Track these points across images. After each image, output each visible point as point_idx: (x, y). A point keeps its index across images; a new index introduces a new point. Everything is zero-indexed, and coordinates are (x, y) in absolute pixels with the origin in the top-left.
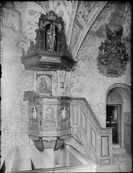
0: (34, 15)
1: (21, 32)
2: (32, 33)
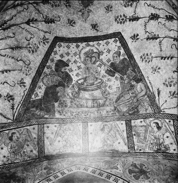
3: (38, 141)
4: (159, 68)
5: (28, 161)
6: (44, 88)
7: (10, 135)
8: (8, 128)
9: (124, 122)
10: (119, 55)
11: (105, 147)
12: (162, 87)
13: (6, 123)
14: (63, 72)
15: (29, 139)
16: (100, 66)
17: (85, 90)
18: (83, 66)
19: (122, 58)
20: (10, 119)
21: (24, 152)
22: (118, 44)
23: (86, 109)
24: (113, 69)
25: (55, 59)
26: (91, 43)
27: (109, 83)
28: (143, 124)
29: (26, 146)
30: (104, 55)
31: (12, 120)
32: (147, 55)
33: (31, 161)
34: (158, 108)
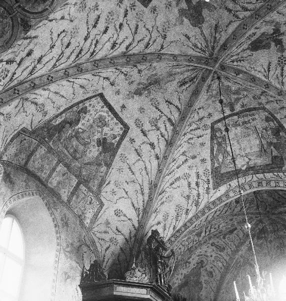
0: (119, 216)
1: (90, 229)
2: (104, 240)
4: (122, 171)
6: (63, 118)
9: (77, 181)
10: (114, 139)
11: (56, 189)
12: (112, 182)
14: (79, 116)
16: (98, 132)
17: (77, 138)
18: (91, 121)
19: (113, 141)
22: (121, 132)
23: (67, 153)
24: (102, 143)
25: (86, 105)
26: (110, 113)
27: (92, 148)
28: (86, 193)
30: (108, 128)
32: (125, 157)
34: (100, 191)
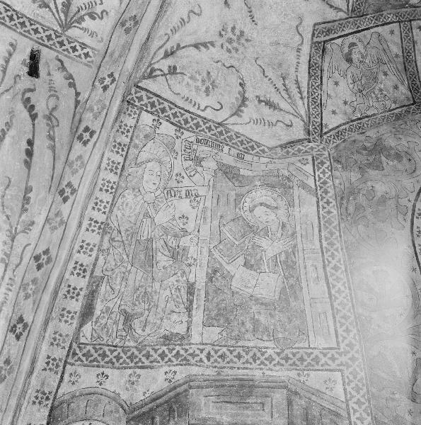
3: (404, 63)
5: (394, 109)
7: (346, 50)
8: (340, 34)
13: (335, 21)
15: (385, 59)
20: (341, 10)
21: (381, 90)
29: (381, 77)
31: (345, 12)
33: (400, 110)
